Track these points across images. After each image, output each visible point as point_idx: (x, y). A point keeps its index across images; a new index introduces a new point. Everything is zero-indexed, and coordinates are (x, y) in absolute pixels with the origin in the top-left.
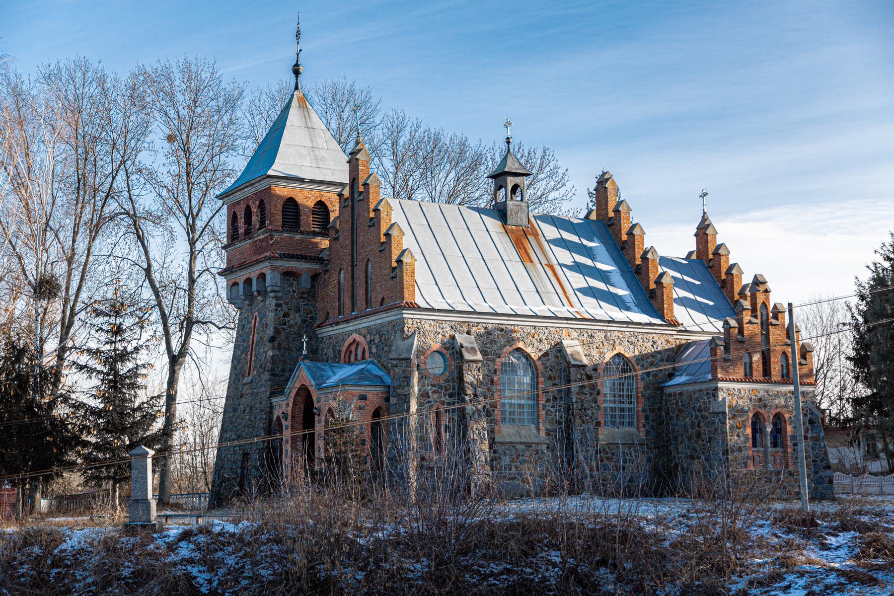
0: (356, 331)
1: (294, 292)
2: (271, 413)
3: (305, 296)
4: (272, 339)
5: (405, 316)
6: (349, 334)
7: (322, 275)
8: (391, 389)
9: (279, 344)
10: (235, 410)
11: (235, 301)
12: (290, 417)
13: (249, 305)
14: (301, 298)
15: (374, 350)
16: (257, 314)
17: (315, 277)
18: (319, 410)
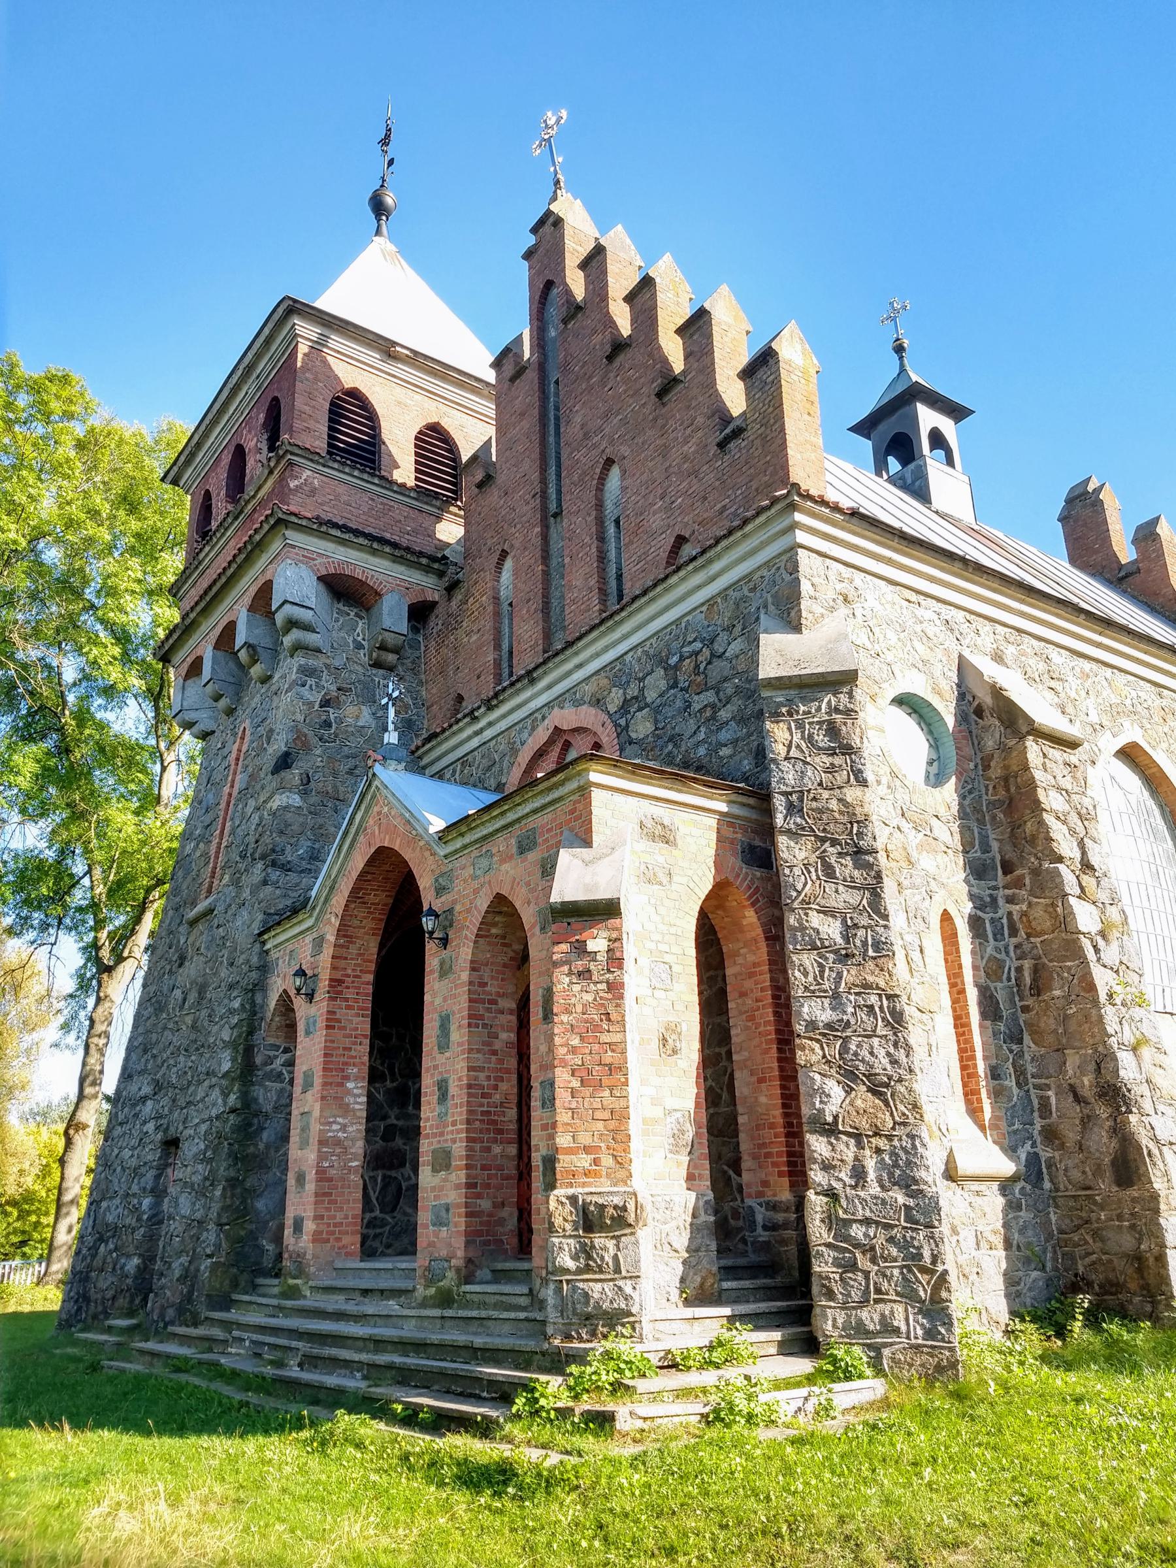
0: (559, 701)
1: (359, 646)
2: (259, 987)
3: (391, 658)
4: (284, 762)
5: (801, 537)
6: (534, 719)
7: (439, 610)
8: (779, 803)
9: (307, 780)
10: (160, 1008)
11: (190, 716)
12: (323, 985)
13: (230, 712)
14: (377, 665)
15: (642, 727)
16: (247, 724)
17: (420, 613)
18: (446, 918)
